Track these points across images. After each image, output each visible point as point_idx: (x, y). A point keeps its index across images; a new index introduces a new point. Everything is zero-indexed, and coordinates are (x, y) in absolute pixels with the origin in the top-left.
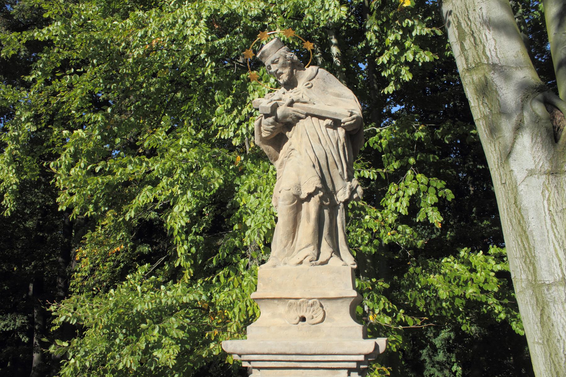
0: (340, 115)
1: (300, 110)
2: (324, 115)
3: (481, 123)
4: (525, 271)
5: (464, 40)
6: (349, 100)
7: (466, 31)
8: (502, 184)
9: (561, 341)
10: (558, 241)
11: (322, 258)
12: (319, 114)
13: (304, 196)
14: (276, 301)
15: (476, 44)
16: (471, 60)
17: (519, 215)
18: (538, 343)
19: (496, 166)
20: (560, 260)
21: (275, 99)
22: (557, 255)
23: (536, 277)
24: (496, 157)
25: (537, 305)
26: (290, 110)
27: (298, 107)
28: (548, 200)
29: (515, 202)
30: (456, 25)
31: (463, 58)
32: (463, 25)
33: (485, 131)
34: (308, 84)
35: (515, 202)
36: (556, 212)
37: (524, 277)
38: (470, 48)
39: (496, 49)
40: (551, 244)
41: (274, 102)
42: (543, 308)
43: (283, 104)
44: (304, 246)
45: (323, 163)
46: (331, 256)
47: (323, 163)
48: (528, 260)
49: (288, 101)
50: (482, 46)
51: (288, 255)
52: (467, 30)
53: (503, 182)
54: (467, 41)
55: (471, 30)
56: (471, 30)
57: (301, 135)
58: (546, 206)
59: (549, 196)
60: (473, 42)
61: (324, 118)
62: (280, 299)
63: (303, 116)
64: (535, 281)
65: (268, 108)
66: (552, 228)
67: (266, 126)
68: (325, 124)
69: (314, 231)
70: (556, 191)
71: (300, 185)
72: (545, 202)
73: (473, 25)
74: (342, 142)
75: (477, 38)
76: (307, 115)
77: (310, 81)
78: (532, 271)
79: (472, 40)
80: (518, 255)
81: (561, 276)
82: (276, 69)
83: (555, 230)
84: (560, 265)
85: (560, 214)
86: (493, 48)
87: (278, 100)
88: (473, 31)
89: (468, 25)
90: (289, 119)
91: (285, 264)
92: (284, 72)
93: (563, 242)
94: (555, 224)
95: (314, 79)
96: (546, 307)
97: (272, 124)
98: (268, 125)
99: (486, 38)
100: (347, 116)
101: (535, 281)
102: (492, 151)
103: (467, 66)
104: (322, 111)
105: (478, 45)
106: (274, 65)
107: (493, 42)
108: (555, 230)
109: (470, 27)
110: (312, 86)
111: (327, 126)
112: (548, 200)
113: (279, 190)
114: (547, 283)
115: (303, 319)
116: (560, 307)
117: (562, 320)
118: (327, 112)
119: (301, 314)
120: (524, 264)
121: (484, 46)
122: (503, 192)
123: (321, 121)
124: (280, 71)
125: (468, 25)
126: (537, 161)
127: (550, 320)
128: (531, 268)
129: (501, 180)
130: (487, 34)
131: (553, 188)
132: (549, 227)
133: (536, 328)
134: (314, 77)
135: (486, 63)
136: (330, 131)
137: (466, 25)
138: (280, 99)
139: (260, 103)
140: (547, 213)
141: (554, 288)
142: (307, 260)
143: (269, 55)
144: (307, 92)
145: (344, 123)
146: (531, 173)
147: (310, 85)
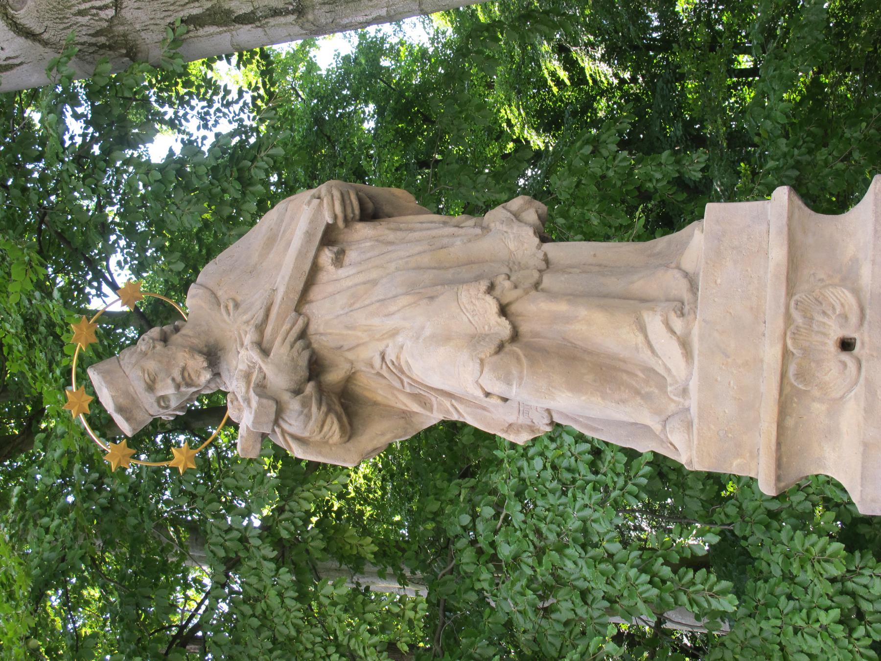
0: (313, 221)
1: (286, 327)
2: (307, 267)
5: (229, 12)
6: (289, 213)
11: (679, 287)
12: (303, 279)
13: (503, 328)
14: (790, 422)
21: (244, 390)
26: (280, 350)
27: (275, 332)
31: (272, 21)
32: (195, 12)
34: (226, 307)
41: (252, 394)
43: (260, 368)
44: (640, 338)
45: (429, 276)
46: (678, 268)
47: (429, 276)
49: (255, 356)
51: (662, 383)
57: (347, 328)
61: (315, 269)
62: (783, 411)
63: (301, 322)
65: (260, 405)
67: (311, 423)
68: (331, 268)
69: (603, 308)
71: (473, 337)
74: (387, 232)
76: (298, 310)
77: (219, 304)
82: (169, 381)
87: (248, 383)
90: (303, 361)
91: (685, 392)
92: (182, 364)
95: (220, 293)
97: (305, 404)
98: (308, 417)
100: (320, 205)
103: (292, 12)
104: (296, 267)
106: (159, 386)
110: (234, 300)
111: (339, 260)
113: (481, 395)
115: (846, 345)
118: (301, 255)
119: (832, 346)
123: (323, 277)
124: (176, 374)
134: (214, 294)
136: (352, 255)
138: (247, 376)
139: (247, 427)
142: (678, 324)
143: (127, 394)
144: (245, 313)
145: (335, 217)
147: (231, 305)
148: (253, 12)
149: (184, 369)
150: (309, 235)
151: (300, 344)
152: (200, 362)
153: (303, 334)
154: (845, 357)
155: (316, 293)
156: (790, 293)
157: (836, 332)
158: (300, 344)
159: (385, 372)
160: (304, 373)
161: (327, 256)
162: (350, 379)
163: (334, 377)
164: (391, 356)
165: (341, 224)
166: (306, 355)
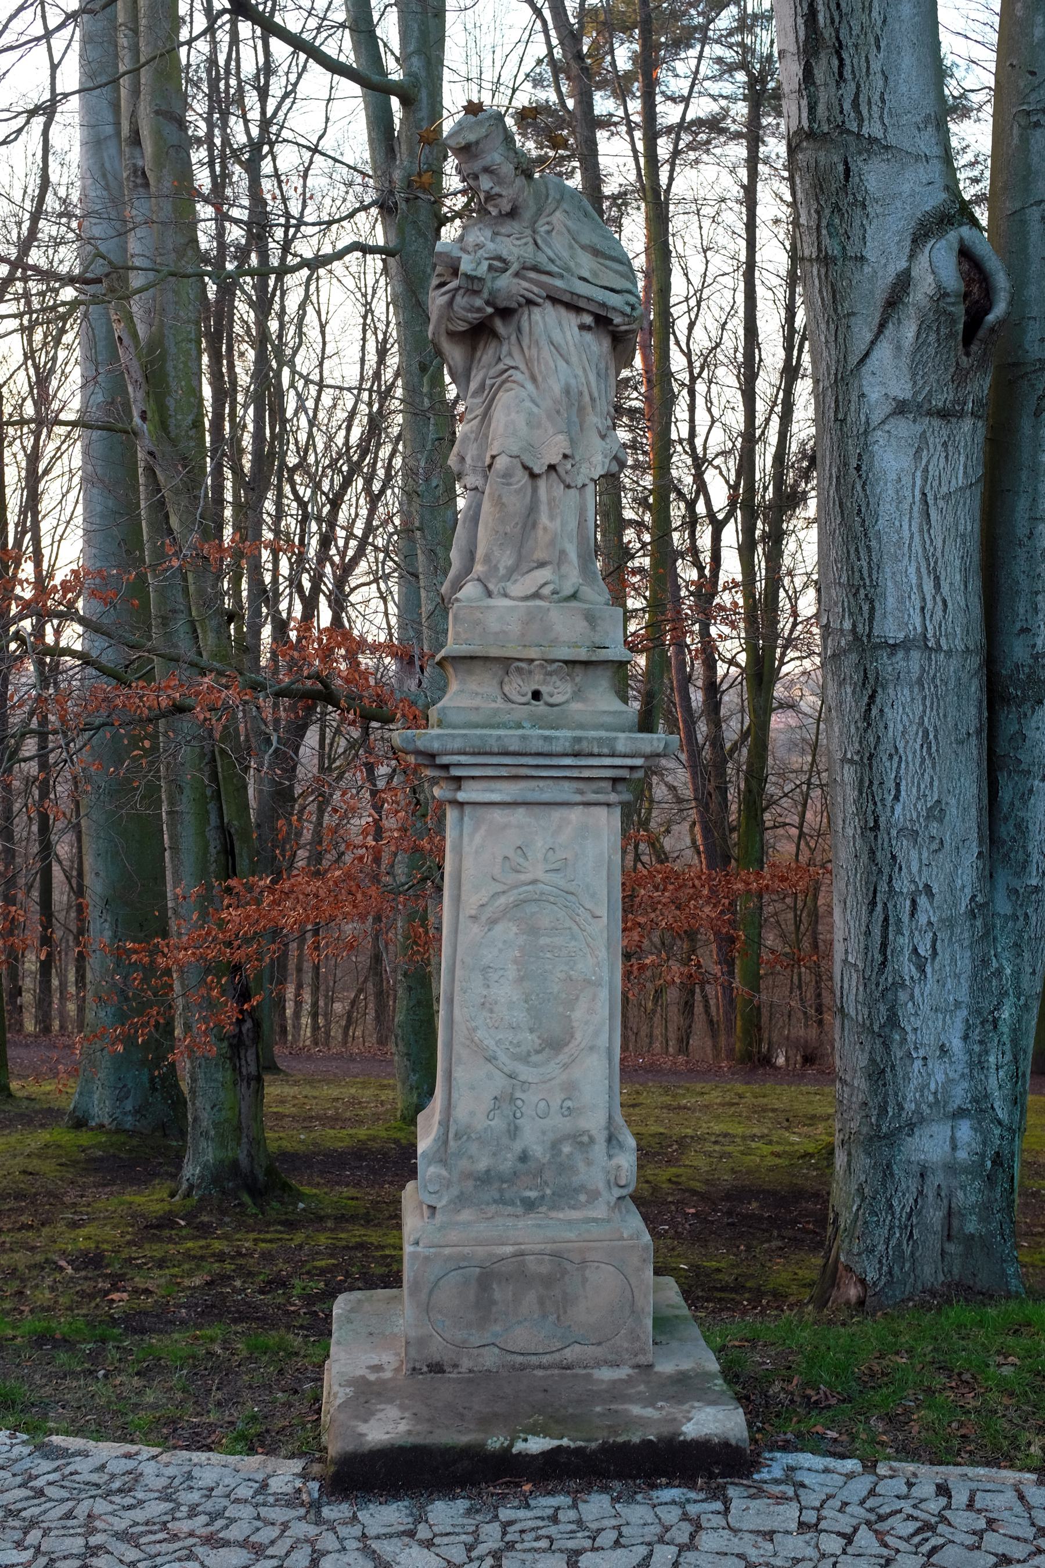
1: (536, 289)
2: (582, 304)
3: (815, 272)
4: (851, 614)
7: (827, 36)
8: (836, 420)
9: (896, 759)
10: (927, 560)
15: (841, 74)
16: (821, 110)
17: (861, 495)
18: (851, 761)
19: (832, 377)
20: (924, 599)
22: (920, 586)
23: (871, 629)
24: (834, 357)
25: (864, 684)
28: (926, 470)
29: (858, 468)
30: (806, 11)
31: (804, 103)
33: (820, 291)
35: (858, 468)
36: (936, 499)
37: (847, 625)
38: (826, 85)
39: (883, 101)
40: (913, 563)
42: (875, 691)
48: (862, 592)
50: (853, 85)
52: (828, 33)
53: (840, 417)
54: (824, 62)
55: (838, 38)
56: (838, 38)
58: (919, 482)
59: (928, 462)
60: (836, 70)
61: (578, 310)
63: (540, 301)
64: (869, 636)
66: (921, 531)
70: (943, 454)
72: (919, 474)
73: (844, 25)
75: (847, 61)
78: (866, 615)
79: (835, 62)
80: (844, 579)
81: (919, 630)
83: (926, 536)
84: (923, 609)
85: (941, 503)
86: (876, 98)
88: (840, 43)
89: (833, 22)
93: (936, 563)
94: (929, 522)
96: (880, 690)
98: (469, 311)
99: (868, 68)
101: (869, 636)
102: (827, 342)
105: (845, 81)
107: (881, 83)
108: (926, 536)
109: (837, 31)
111: (583, 327)
112: (926, 470)
113: (494, 453)
114: (891, 642)
116: (906, 691)
117: (905, 717)
120: (852, 600)
121: (858, 86)
122: (835, 439)
125: (833, 22)
126: (920, 383)
127: (882, 716)
128: (866, 608)
129: (836, 412)
130: (871, 57)
131: (939, 447)
132: (915, 529)
133: (853, 730)
135: (856, 130)
136: (588, 337)
137: (828, 21)
140: (917, 498)
141: (900, 654)
145: (617, 326)
146: (901, 408)
148: (814, 83)
149: (500, 196)
150: (604, 305)
151: (521, 299)
152: (507, 208)
153: (530, 302)
154: (530, 695)
155: (562, 311)
156: (566, 662)
157: (543, 689)
158: (521, 299)
159: (501, 366)
160: (502, 304)
161: (588, 319)
162: (495, 335)
163: (499, 325)
164: (517, 376)
165: (611, 328)
166: (514, 305)
